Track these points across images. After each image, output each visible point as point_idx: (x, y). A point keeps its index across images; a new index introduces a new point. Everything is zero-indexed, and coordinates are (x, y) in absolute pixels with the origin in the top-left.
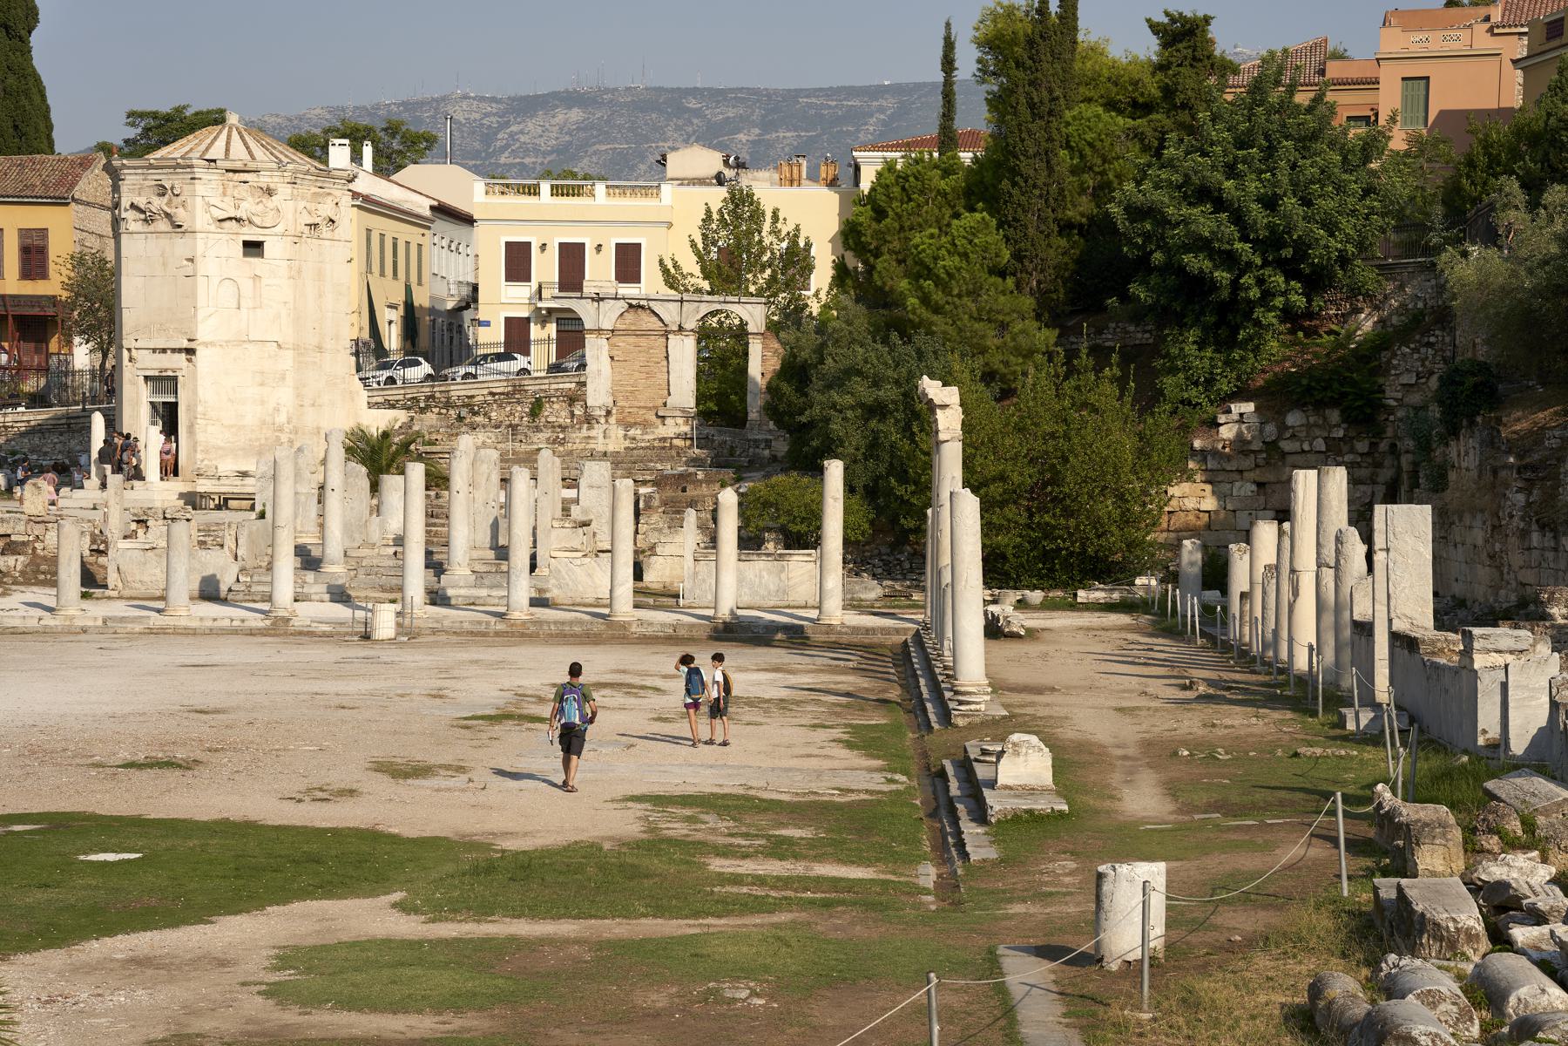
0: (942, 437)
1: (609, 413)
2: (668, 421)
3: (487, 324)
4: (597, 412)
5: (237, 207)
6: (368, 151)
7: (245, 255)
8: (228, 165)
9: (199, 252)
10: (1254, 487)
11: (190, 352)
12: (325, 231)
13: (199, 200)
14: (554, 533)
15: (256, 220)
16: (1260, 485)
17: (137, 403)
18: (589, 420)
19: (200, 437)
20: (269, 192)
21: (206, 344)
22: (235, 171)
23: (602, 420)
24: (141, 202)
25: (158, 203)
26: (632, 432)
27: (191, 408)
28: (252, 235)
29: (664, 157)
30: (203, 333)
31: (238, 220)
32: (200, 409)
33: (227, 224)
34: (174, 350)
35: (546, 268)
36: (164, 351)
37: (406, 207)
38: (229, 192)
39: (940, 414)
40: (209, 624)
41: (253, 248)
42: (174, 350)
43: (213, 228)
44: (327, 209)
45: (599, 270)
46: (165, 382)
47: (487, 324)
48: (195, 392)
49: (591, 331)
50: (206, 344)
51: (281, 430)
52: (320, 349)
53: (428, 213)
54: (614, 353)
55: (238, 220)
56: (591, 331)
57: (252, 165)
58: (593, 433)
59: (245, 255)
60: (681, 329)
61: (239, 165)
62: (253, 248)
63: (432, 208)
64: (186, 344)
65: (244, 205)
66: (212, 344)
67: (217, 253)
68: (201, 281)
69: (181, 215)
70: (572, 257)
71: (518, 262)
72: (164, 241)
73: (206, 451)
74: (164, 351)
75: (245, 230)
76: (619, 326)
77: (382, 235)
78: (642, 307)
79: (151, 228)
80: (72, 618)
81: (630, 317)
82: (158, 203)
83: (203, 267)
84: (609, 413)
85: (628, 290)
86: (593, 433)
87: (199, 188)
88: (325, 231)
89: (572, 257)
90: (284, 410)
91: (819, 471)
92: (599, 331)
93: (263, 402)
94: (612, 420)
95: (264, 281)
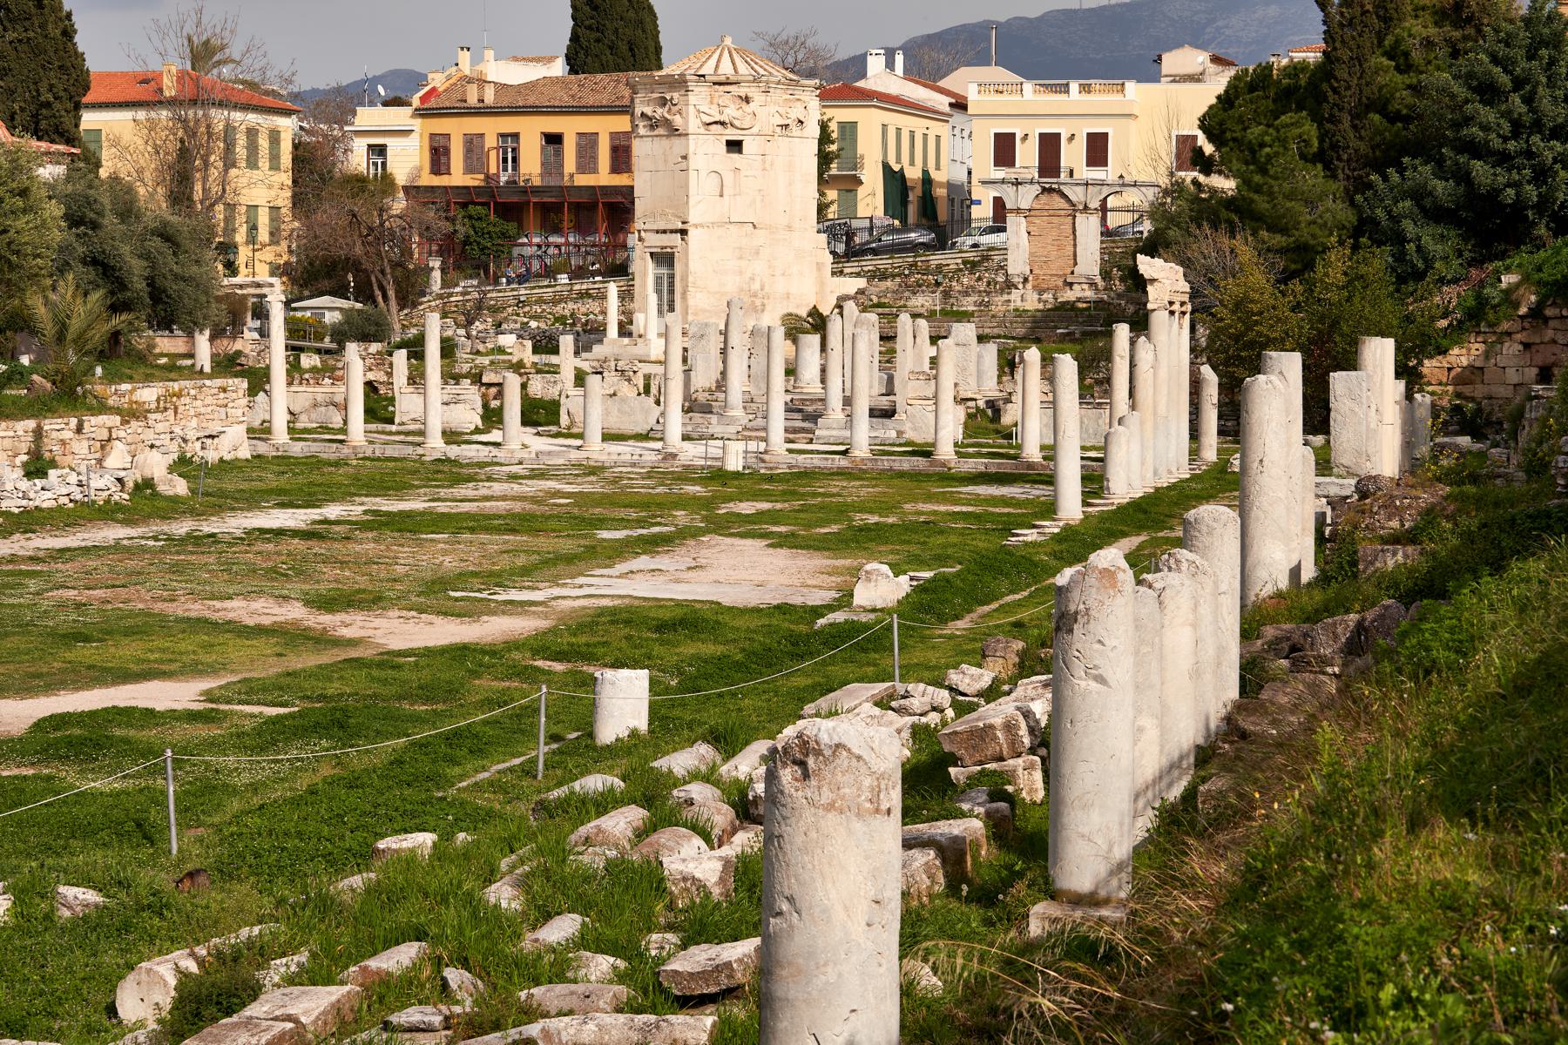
0: (1150, 306)
1: (1026, 280)
2: (1076, 287)
3: (979, 202)
4: (1016, 280)
5: (721, 113)
6: (899, 59)
7: (729, 151)
8: (715, 79)
9: (691, 150)
10: (1521, 347)
11: (684, 232)
12: (795, 130)
13: (691, 108)
14: (911, 384)
15: (736, 123)
16: (1527, 346)
17: (645, 274)
18: (1009, 285)
19: (691, 302)
20: (747, 100)
21: (696, 226)
22: (720, 84)
24: (648, 111)
25: (660, 112)
26: (1045, 296)
27: (685, 279)
28: (733, 135)
29: (1160, 57)
30: (694, 216)
31: (722, 123)
32: (691, 279)
34: (672, 231)
35: (1027, 156)
36: (664, 232)
37: (929, 104)
39: (1149, 288)
40: (615, 457)
41: (735, 146)
42: (672, 231)
43: (702, 130)
44: (796, 112)
45: (1073, 155)
46: (665, 259)
47: (979, 202)
48: (687, 265)
49: (1011, 211)
50: (696, 226)
51: (755, 296)
52: (789, 228)
53: (947, 109)
55: (722, 123)
56: (1011, 211)
57: (733, 79)
59: (729, 151)
60: (1086, 207)
61: (723, 79)
62: (735, 146)
63: (951, 105)
64: (680, 226)
65: (727, 111)
66: (702, 226)
67: (705, 150)
68: (692, 174)
69: (677, 121)
70: (1050, 145)
71: (1004, 149)
72: (665, 142)
73: (696, 314)
74: (664, 232)
77: (899, 129)
80: (512, 452)
81: (1044, 198)
82: (660, 112)
83: (694, 162)
84: (1026, 280)
85: (1096, 174)
87: (692, 98)
88: (795, 130)
89: (1050, 145)
90: (758, 280)
91: (1110, 334)
92: (1018, 211)
93: (741, 273)
94: (1029, 286)
95: (743, 173)
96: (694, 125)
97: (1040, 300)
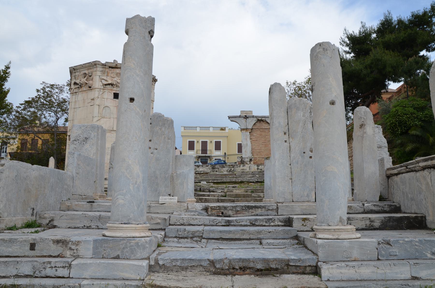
1: (251, 160)
23: (249, 163)
24: (78, 81)
25: (84, 80)
33: (108, 86)
35: (198, 147)
38: (109, 75)
45: (211, 147)
54: (252, 137)
55: (112, 85)
58: (245, 168)
65: (115, 79)
70: (204, 144)
75: (115, 89)
76: (253, 128)
78: (262, 121)
79: (81, 90)
81: (258, 124)
82: (84, 80)
86: (245, 168)
89: (204, 144)
94: (252, 163)
96: (97, 83)
97: (258, 169)
